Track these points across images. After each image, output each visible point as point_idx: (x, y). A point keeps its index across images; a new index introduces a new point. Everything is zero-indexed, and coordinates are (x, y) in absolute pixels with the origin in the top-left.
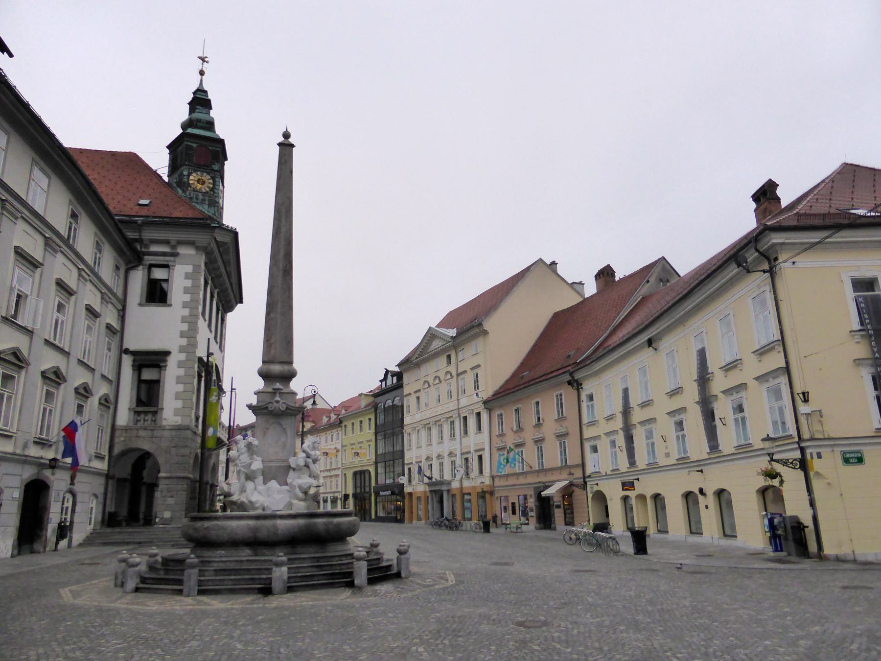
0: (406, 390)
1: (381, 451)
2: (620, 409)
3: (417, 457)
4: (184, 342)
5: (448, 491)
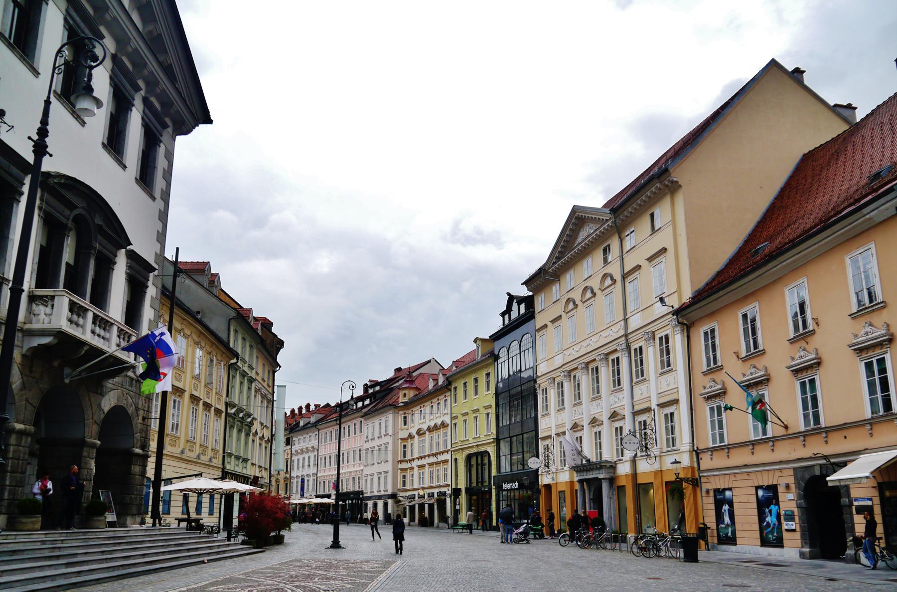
0: (540, 320)
1: (505, 421)
3: (557, 426)
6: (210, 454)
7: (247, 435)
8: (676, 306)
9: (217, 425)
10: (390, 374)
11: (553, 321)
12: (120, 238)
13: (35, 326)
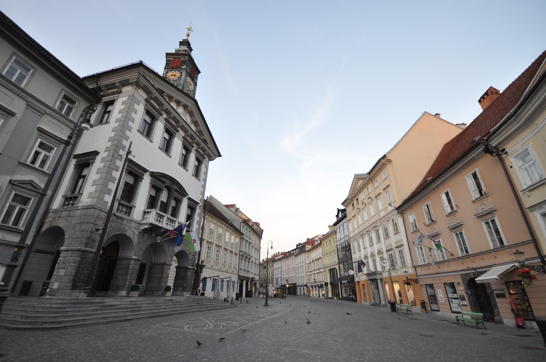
0: (349, 217)
1: (341, 256)
5: (381, 279)
6: (232, 269)
7: (249, 262)
9: (234, 260)
10: (305, 241)
11: (353, 217)
12: (183, 193)
13: (144, 222)
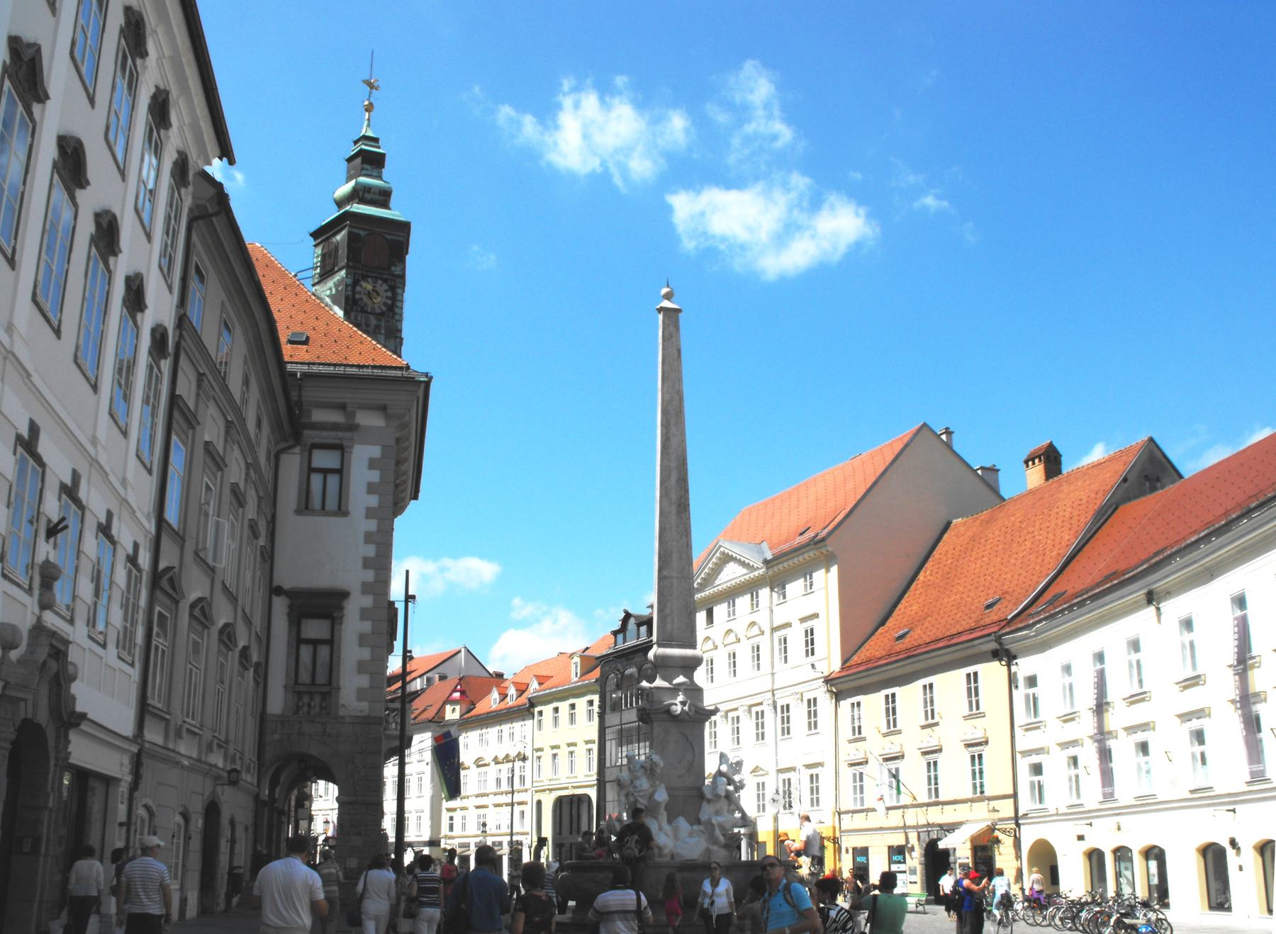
2: (1092, 703)
4: (369, 576)
8: (826, 674)
